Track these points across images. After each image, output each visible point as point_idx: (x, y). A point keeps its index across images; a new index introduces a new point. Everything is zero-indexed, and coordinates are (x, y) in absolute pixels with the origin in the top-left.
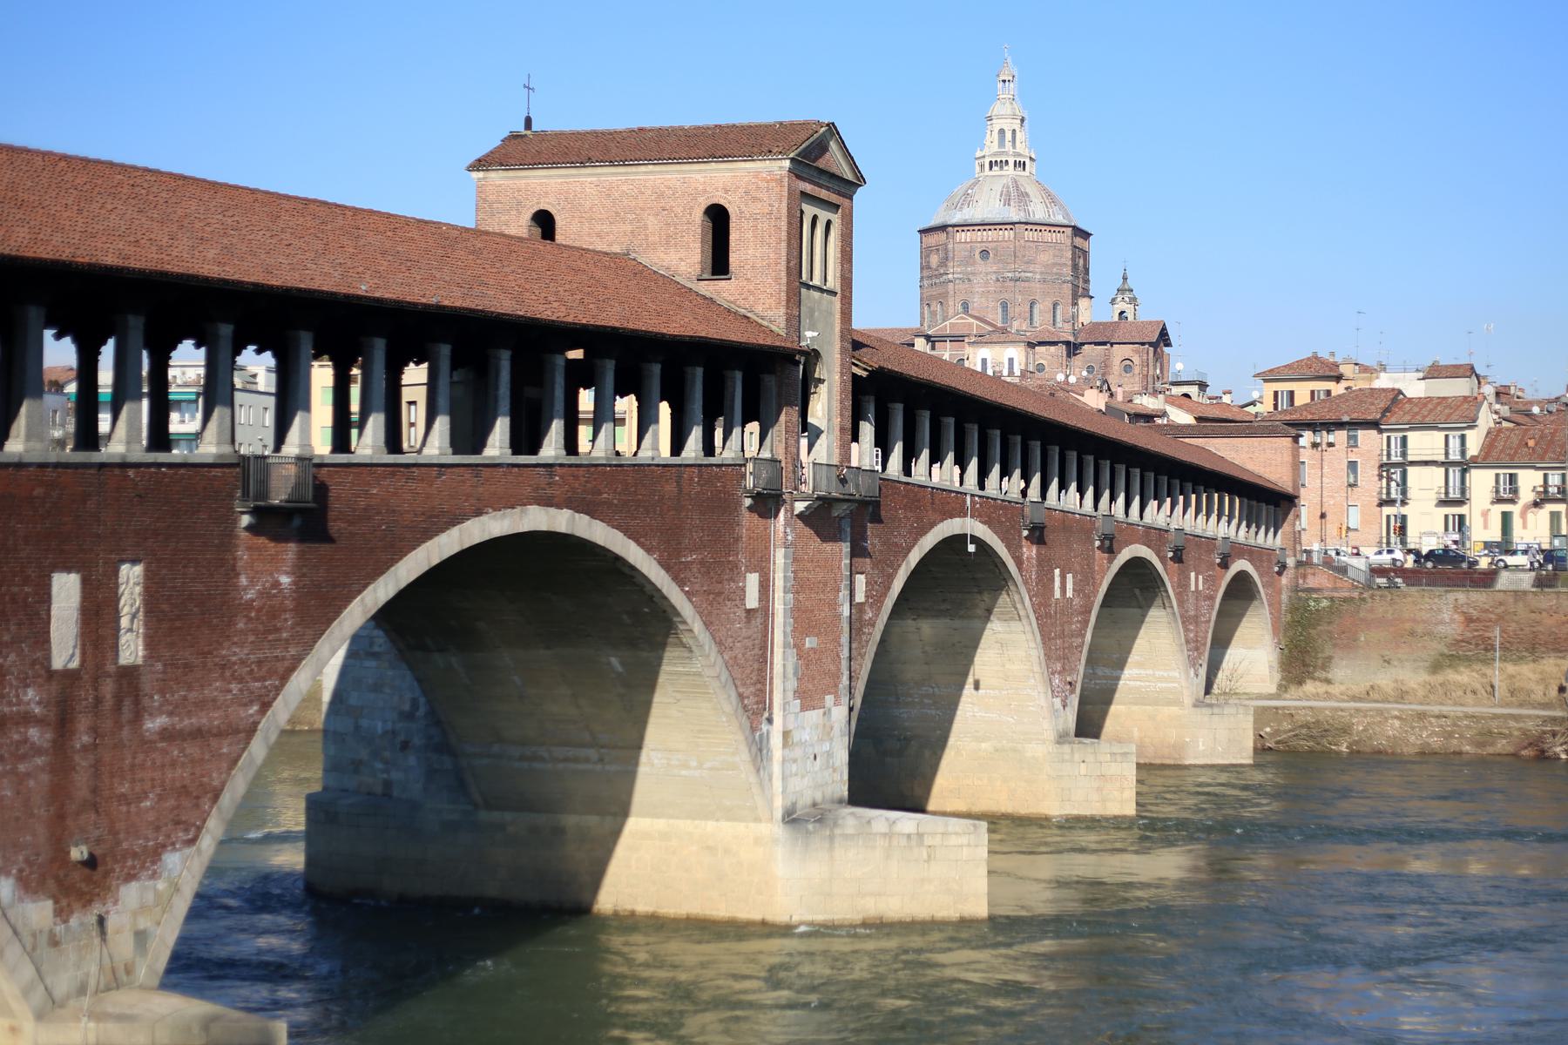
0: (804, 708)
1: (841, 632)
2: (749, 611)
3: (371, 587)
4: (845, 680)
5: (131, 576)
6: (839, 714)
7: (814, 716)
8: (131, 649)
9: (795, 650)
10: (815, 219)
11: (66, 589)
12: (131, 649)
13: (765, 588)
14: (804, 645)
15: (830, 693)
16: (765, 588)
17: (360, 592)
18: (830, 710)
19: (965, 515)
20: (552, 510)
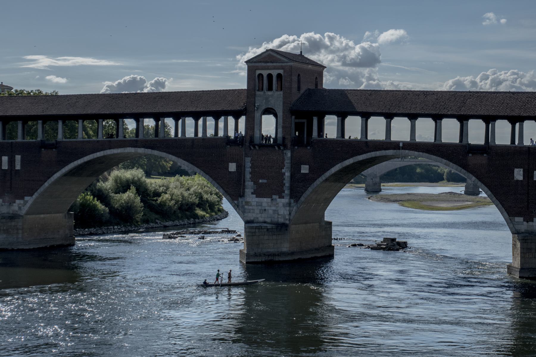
0: (256, 197)
1: (284, 179)
2: (231, 172)
3: (76, 161)
4: (287, 192)
5: (18, 158)
6: (285, 200)
7: (265, 199)
8: (18, 167)
9: (253, 182)
10: (270, 76)
11: (5, 159)
12: (18, 167)
13: (237, 167)
14: (259, 181)
15: (275, 195)
16: (240, 167)
17: (73, 161)
18: (276, 199)
19: (399, 149)
20: (136, 149)
